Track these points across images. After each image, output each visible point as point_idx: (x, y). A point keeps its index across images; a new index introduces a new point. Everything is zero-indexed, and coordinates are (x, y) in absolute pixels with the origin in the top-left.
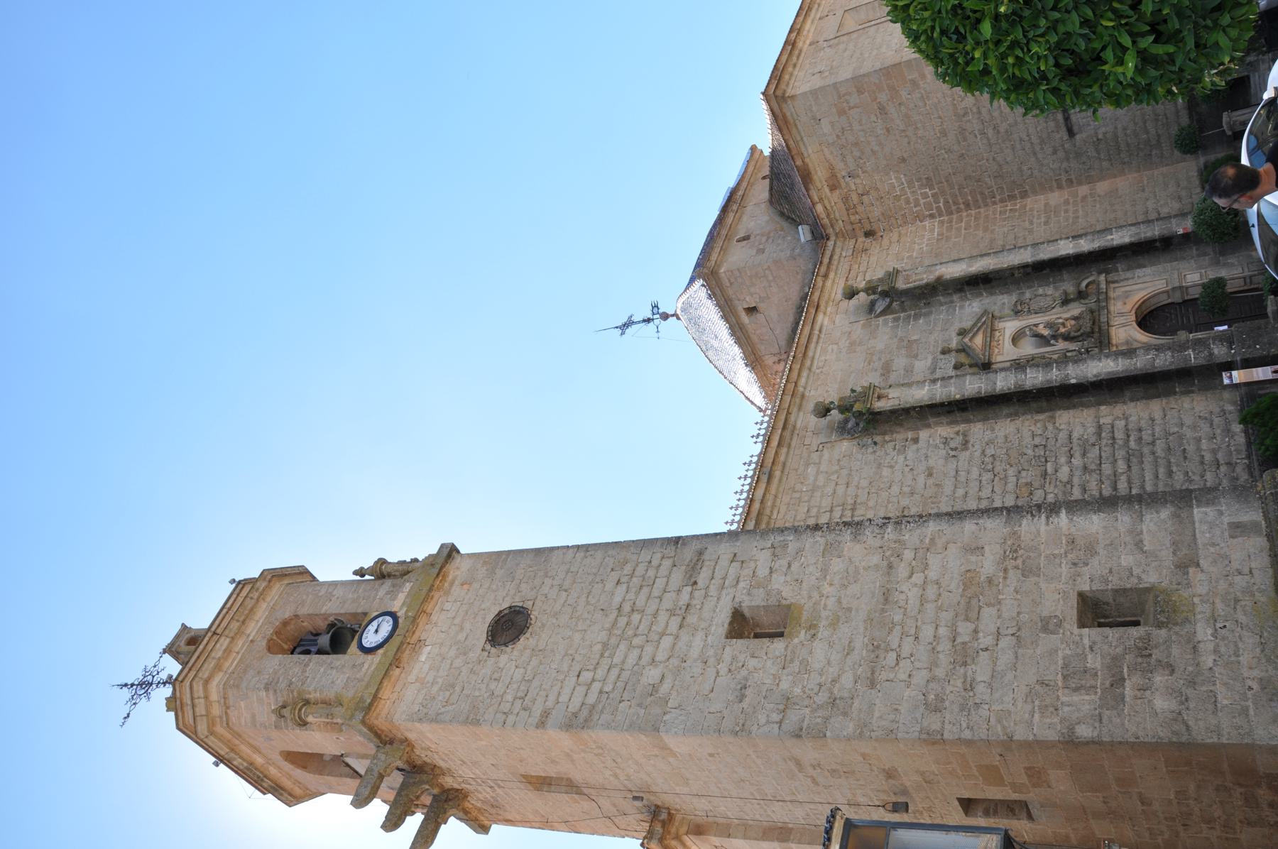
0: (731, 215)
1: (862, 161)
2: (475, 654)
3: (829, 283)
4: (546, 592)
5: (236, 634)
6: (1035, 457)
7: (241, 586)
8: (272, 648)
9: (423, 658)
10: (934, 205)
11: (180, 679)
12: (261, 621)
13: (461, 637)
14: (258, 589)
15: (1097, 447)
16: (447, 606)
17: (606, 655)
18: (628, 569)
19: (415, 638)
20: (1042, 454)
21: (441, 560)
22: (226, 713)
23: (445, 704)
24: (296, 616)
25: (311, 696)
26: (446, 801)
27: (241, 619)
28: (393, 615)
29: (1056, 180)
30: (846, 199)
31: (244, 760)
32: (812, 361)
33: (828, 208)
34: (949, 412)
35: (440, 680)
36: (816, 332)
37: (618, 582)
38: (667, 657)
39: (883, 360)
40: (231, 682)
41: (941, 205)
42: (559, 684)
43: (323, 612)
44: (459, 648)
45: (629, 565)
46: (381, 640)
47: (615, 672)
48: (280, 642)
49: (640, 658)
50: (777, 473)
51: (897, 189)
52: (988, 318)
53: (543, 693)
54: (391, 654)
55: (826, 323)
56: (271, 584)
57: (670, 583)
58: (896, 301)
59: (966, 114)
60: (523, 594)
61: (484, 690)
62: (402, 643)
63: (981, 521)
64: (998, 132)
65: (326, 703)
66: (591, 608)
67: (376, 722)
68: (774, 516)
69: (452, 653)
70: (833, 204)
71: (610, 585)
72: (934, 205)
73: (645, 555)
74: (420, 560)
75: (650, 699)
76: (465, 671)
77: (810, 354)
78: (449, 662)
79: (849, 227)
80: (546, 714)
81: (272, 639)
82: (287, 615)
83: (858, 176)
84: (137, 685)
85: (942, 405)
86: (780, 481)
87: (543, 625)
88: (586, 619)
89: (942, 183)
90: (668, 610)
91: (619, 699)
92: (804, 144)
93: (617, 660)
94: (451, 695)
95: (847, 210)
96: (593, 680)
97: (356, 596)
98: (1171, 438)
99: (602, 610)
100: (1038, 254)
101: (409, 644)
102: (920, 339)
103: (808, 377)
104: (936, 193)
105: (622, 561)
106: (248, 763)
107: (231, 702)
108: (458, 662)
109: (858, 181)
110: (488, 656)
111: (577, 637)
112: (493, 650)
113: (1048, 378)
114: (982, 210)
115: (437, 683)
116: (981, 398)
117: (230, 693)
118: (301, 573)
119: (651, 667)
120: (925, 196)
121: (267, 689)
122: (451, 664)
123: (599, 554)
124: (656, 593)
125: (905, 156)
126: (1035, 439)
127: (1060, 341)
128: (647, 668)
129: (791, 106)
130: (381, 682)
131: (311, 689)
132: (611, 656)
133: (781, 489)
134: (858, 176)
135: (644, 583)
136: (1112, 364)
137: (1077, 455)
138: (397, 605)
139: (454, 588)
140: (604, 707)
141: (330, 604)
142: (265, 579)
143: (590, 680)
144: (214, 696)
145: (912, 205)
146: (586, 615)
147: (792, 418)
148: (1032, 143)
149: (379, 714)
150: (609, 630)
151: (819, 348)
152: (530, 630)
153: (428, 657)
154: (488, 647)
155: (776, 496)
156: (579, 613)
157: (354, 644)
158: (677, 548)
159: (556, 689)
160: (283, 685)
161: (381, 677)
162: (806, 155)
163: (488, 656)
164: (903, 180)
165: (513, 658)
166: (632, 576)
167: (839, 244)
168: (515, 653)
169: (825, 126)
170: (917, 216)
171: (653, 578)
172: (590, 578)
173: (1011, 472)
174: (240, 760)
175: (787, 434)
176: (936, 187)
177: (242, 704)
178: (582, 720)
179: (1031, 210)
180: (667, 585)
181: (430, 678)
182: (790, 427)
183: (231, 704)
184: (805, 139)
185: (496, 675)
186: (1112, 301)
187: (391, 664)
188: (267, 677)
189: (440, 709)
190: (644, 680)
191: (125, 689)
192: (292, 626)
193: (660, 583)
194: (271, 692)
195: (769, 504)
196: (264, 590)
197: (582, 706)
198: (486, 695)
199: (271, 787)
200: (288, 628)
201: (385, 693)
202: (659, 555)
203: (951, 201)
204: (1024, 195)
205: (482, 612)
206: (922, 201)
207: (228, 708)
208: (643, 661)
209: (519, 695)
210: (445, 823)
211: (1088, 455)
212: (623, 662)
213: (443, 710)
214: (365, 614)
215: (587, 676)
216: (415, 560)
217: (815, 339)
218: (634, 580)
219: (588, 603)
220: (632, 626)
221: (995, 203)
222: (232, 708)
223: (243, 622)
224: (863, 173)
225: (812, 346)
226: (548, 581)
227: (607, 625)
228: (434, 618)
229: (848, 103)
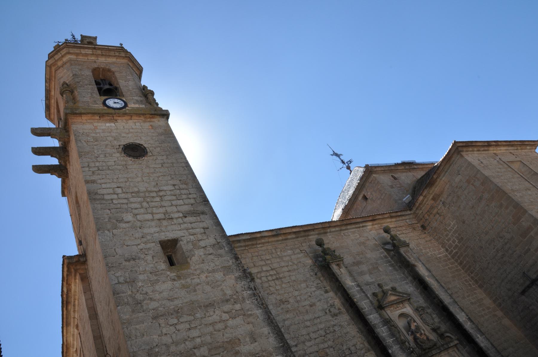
0: (403, 167)
1: (452, 204)
2: (116, 143)
3: (389, 220)
4: (159, 158)
5: (95, 55)
6: (343, 351)
7: (121, 48)
8: (95, 71)
9: (108, 125)
10: (452, 248)
11: (68, 44)
12: (107, 62)
13: (123, 135)
14: (120, 54)
16: (138, 124)
17: (133, 194)
18: (184, 186)
19: (117, 118)
20: (347, 354)
21: (159, 112)
22: (60, 67)
23: (86, 141)
24: (114, 73)
25: (76, 93)
26: (61, 170)
27: (103, 54)
28: (126, 105)
29: (496, 298)
30: (432, 207)
31: (49, 87)
33: (424, 202)
34: (346, 300)
35: (98, 135)
36: (361, 225)
37: (174, 185)
38: (140, 219)
39: (362, 260)
40: (72, 62)
41: (454, 251)
42: (111, 181)
43: (119, 81)
44: (117, 136)
45: (185, 186)
46: (115, 107)
47: (125, 201)
48: (101, 73)
49: (136, 209)
50: (280, 238)
51: (449, 228)
52: (406, 297)
53: (104, 176)
54: (104, 111)
55: (368, 227)
56: (125, 58)
57: (182, 206)
58: (394, 252)
59: (501, 238)
60: (154, 150)
61: (99, 153)
62: (111, 114)
63: (271, 335)
64: (502, 258)
65: (74, 99)
66: (156, 179)
67: (70, 120)
68: (258, 246)
69: (114, 134)
70: (427, 203)
71: (171, 182)
72: (452, 248)
73: (192, 191)
74: (159, 106)
75: (114, 221)
76: (106, 142)
77: (349, 227)
78: (109, 135)
79: (421, 217)
80: (93, 182)
81: (99, 69)
82: (113, 69)
83: (445, 207)
84: (75, 40)
85: (348, 295)
86: (278, 241)
87: (141, 164)
88: (149, 179)
89: (464, 246)
90: (166, 211)
91: (111, 208)
92: (445, 174)
93: (132, 200)
94: (92, 142)
95: (428, 211)
96: (117, 194)
97: (131, 89)
99: (157, 184)
100: (451, 305)
101: (113, 117)
102: (381, 272)
104: (458, 246)
105: (187, 182)
106: (49, 89)
107: (65, 66)
108: (110, 138)
109: (443, 208)
110: (116, 149)
111: (139, 179)
112: (120, 149)
113: (386, 338)
114: (462, 271)
115: (97, 134)
116: (360, 311)
117: (68, 64)
118: (138, 69)
119: (132, 215)
120: (454, 242)
121: (73, 75)
122: (108, 136)
123: (186, 172)
124: (174, 203)
125: (466, 222)
126: (353, 347)
127: (412, 336)
128: (131, 214)
129: (458, 158)
130: (88, 113)
131: (79, 90)
132: (133, 197)
133: (274, 243)
134: (445, 207)
135: (177, 196)
138: (131, 105)
139: (148, 123)
140: (104, 204)
141: (123, 82)
142: (126, 54)
143: (117, 193)
144: (65, 59)
145: (447, 238)
146: (151, 179)
147: (312, 233)
148: (507, 277)
149: (73, 119)
150: (147, 191)
151: (354, 230)
152: (136, 160)
153: (109, 126)
154: (122, 147)
155: (268, 242)
156: (152, 175)
157: (104, 98)
158: (202, 202)
159: (108, 181)
160: (77, 80)
161: (91, 112)
162: (440, 178)
163: (116, 149)
164: (455, 228)
165: (119, 158)
166: (180, 189)
167: (411, 216)
168: (122, 158)
169: (457, 179)
170: (443, 244)
171: (182, 198)
172: (173, 173)
173: (330, 343)
174: (48, 85)
175: (303, 234)
176: (461, 244)
177: (65, 71)
178: (94, 197)
179: (475, 293)
180: (180, 205)
181: (98, 131)
182: (307, 234)
183: (64, 67)
184: (447, 173)
185: (107, 155)
186: (446, 353)
187: (99, 113)
188: (79, 73)
189: (83, 140)
190: (124, 215)
191: (72, 37)
192: (110, 74)
193: (181, 202)
194: (72, 78)
195: (263, 241)
196: (121, 56)
197: (102, 194)
198: (96, 155)
199: (47, 105)
200: (108, 73)
201: (84, 118)
202: (195, 196)
203: (458, 254)
204: (481, 286)
205: (140, 138)
206: (451, 242)
207: (62, 67)
208: (134, 211)
209: (100, 167)
210: (51, 175)
212: (131, 203)
213: (83, 142)
214: (123, 96)
215: (119, 191)
216: (157, 104)
217: (358, 226)
218: (178, 191)
219: (158, 177)
220: (152, 199)
221: (469, 275)
222: (62, 68)
223: (102, 55)
224: (448, 208)
225: (354, 226)
226: (165, 157)
227: (149, 189)
228: (130, 121)
229: (474, 182)
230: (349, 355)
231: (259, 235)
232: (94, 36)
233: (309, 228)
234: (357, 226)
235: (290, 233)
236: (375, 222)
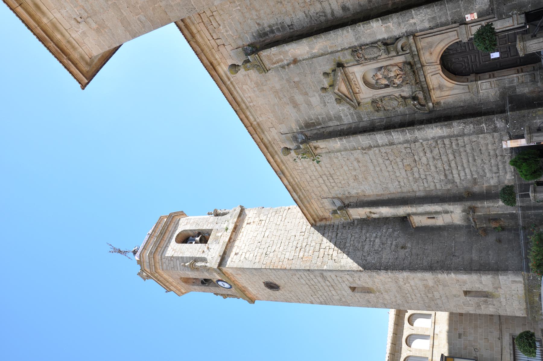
3: (198, 37)
6: (407, 153)
15: (437, 148)
20: (410, 152)
32: (244, 103)
36: (229, 83)
50: (283, 167)
63: (423, 274)
77: (239, 99)
98: (473, 144)
103: (251, 112)
113: (406, 138)
133: (290, 170)
136: (440, 131)
137: (428, 152)
147: (266, 140)
151: (238, 89)
173: (398, 160)
175: (271, 149)
182: (269, 145)
195: (292, 180)
211: (433, 152)
217: (231, 86)
225: (235, 93)
230: (411, 150)
231: (290, 187)
232: (138, 276)
233: (263, 146)
234: (233, 89)
235: (276, 162)
236: (215, 62)
